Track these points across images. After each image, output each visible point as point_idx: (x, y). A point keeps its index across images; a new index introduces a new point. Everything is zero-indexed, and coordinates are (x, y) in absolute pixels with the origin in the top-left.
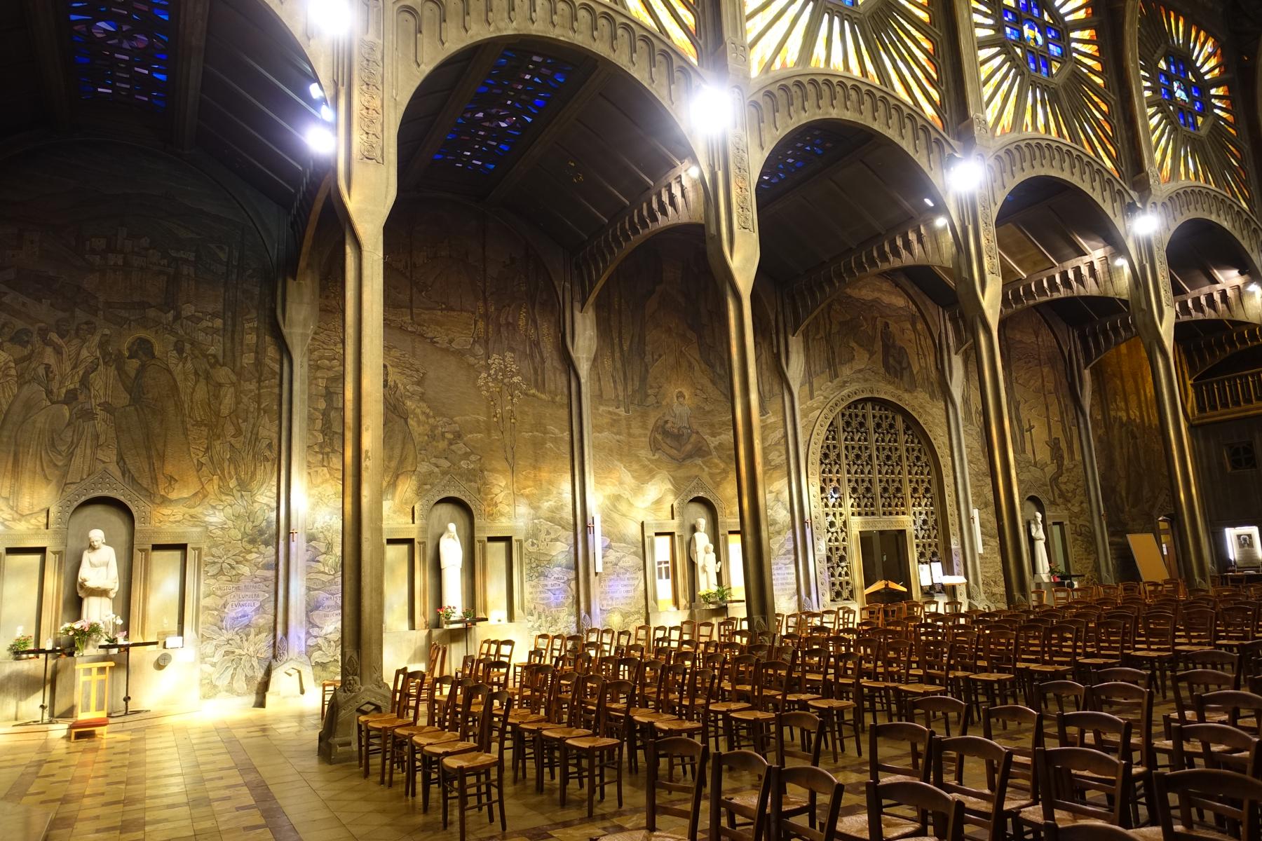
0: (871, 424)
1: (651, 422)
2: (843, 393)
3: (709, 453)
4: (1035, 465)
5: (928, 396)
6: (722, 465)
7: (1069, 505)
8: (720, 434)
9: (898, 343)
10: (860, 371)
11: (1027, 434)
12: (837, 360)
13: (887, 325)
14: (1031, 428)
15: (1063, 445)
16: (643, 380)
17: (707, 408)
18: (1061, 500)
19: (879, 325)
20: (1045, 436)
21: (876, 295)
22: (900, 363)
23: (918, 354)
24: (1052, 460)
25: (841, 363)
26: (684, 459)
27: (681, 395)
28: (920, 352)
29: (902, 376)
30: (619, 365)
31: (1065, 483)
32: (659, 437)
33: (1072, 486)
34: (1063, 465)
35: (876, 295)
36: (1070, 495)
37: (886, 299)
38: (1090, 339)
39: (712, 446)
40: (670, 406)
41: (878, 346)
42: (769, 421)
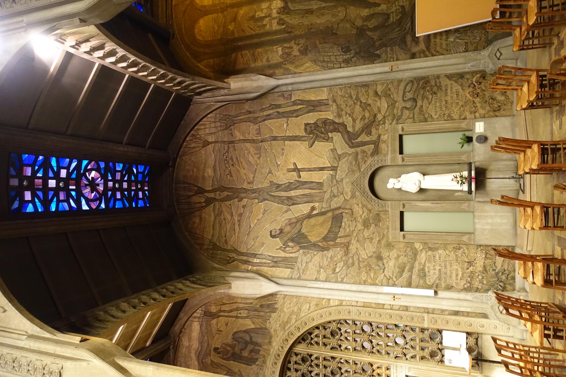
4: (334, 169)
5: (273, 315)
7: (380, 117)
9: (229, 340)
11: (305, 176)
13: (216, 349)
14: (297, 170)
15: (312, 118)
18: (374, 131)
20: (302, 146)
21: (193, 352)
22: (247, 343)
23: (237, 317)
24: (328, 139)
28: (234, 314)
29: (257, 344)
31: (354, 121)
33: (358, 108)
34: (334, 123)
35: (193, 355)
36: (367, 115)
37: (195, 345)
38: (198, 91)
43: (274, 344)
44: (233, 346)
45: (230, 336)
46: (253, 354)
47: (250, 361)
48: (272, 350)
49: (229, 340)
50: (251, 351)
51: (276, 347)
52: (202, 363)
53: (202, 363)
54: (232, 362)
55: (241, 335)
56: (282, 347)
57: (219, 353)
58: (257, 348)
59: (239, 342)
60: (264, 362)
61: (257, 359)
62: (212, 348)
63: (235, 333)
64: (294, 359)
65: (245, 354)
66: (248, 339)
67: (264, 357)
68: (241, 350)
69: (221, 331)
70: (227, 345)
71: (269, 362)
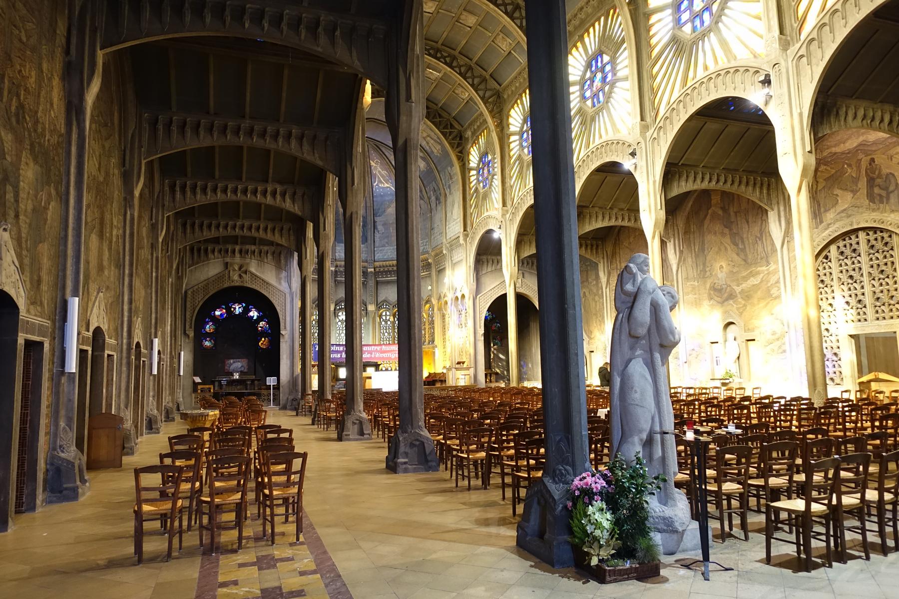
0: (863, 248)
1: (708, 286)
2: (824, 234)
3: (736, 296)
6: (743, 302)
8: (742, 284)
9: (885, 171)
10: (843, 211)
12: (822, 210)
13: (873, 160)
16: (704, 264)
17: (734, 271)
19: (864, 164)
22: (886, 189)
25: (826, 211)
26: (723, 302)
27: (721, 267)
29: (888, 198)
30: (694, 260)
32: (712, 292)
35: (861, 139)
39: (737, 292)
40: (716, 275)
41: (863, 183)
42: (771, 269)
43: (892, 215)
44: (880, 176)
45: (888, 171)
46: (878, 198)
47: (871, 197)
48: (886, 215)
49: (885, 171)
50: (880, 196)
51: (889, 219)
52: (857, 150)
53: (857, 150)
54: (865, 179)
55: (893, 181)
56: (891, 224)
57: (870, 164)
58: (885, 200)
59: (885, 181)
60: (874, 210)
61: (875, 203)
62: (873, 156)
63: (893, 175)
64: (885, 235)
65: (876, 190)
66: (892, 188)
67: (878, 209)
68: (879, 186)
69: (891, 160)
70: (880, 170)
71: (876, 215)
